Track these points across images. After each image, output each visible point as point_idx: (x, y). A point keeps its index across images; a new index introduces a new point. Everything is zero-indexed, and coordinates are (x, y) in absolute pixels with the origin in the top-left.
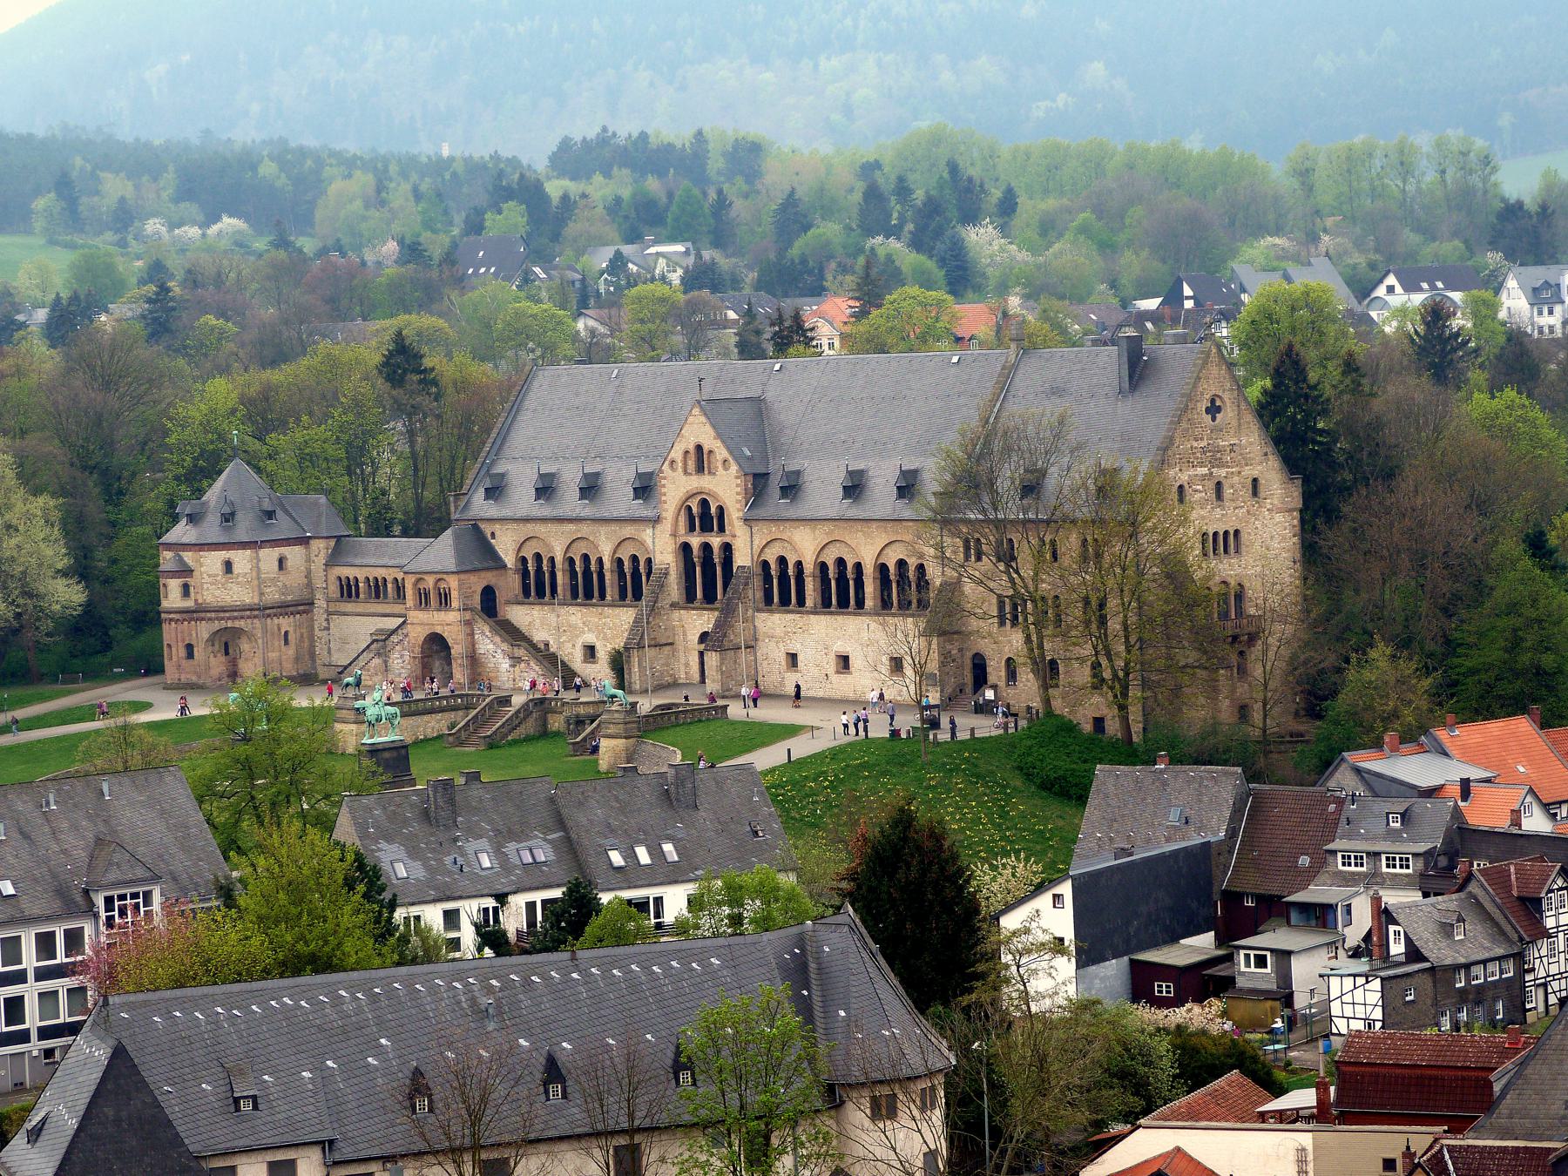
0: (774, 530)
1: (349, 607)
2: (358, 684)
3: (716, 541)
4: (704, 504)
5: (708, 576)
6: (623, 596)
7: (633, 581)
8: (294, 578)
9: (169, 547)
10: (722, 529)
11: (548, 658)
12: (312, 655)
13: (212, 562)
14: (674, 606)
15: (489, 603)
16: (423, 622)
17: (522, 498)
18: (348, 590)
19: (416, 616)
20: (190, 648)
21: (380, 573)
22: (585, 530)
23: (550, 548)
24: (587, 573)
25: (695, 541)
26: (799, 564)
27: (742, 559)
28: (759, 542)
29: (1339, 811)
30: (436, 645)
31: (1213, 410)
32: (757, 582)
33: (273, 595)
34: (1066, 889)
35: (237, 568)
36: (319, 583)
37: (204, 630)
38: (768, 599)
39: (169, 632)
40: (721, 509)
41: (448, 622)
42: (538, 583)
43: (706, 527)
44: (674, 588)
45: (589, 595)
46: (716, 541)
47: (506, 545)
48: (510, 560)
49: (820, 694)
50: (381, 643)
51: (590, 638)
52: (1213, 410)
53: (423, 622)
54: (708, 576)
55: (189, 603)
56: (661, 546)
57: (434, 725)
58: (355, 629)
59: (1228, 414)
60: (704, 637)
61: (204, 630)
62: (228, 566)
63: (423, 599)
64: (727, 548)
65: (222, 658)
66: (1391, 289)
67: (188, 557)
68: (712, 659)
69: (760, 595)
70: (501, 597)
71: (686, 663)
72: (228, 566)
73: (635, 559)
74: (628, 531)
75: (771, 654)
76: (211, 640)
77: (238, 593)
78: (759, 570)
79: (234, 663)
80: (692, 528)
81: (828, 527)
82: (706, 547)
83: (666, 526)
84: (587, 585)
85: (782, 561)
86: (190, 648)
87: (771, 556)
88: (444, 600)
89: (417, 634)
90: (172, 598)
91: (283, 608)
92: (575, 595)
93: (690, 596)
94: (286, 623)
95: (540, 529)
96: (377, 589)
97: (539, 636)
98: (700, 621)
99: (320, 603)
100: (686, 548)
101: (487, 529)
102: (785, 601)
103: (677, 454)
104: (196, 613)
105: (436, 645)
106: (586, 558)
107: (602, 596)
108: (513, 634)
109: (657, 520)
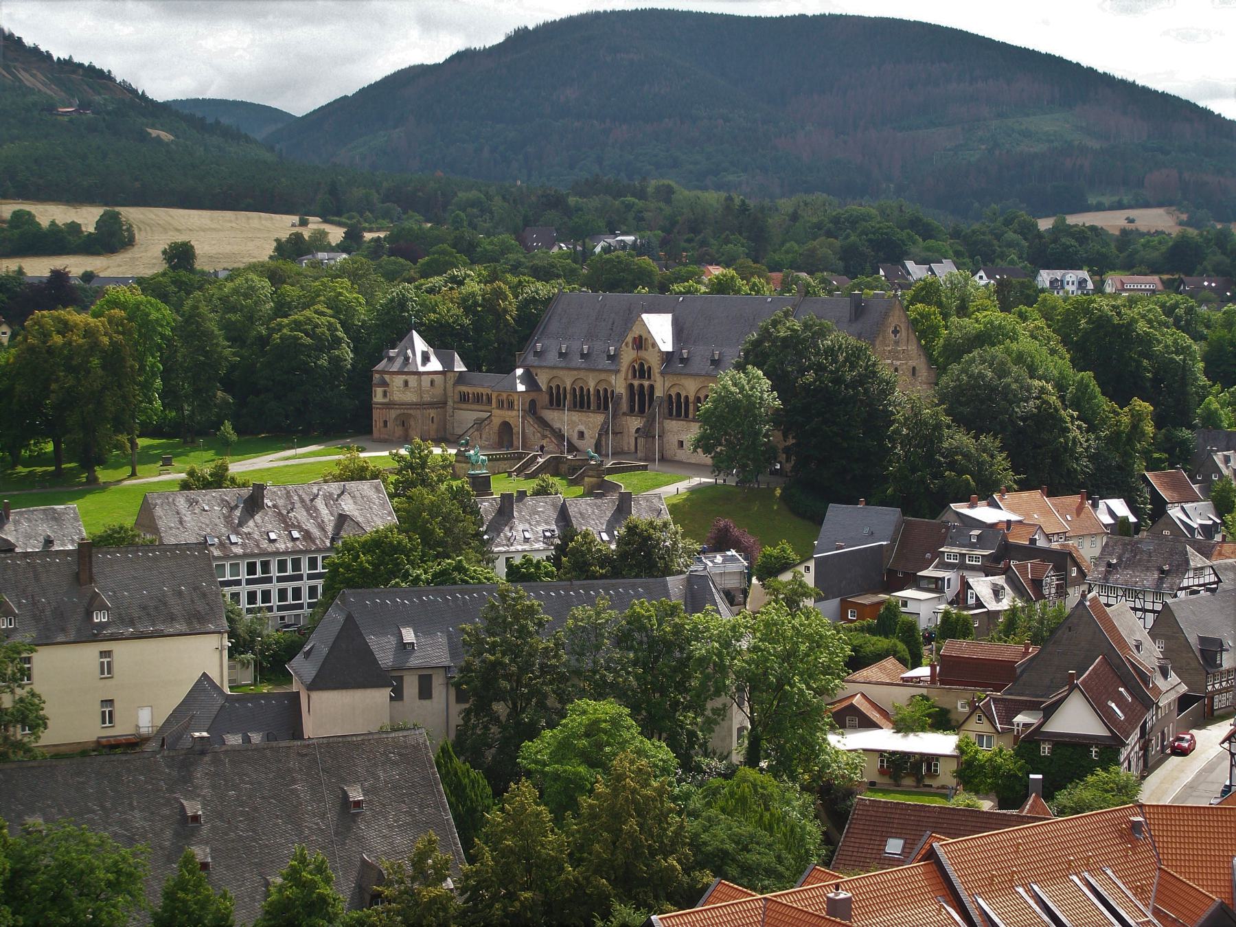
0: (675, 380)
1: (464, 406)
2: (467, 444)
3: (646, 383)
4: (642, 365)
5: (641, 400)
6: (599, 408)
7: (604, 401)
8: (438, 391)
9: (378, 372)
10: (649, 377)
11: (559, 436)
12: (445, 429)
13: (398, 381)
14: (624, 414)
15: (532, 409)
16: (499, 416)
17: (552, 358)
18: (464, 398)
19: (496, 412)
20: (385, 422)
21: (480, 390)
22: (582, 374)
23: (564, 382)
24: (582, 395)
25: (636, 383)
26: (687, 397)
27: (658, 393)
28: (667, 385)
29: (947, 532)
30: (506, 428)
31: (895, 332)
32: (665, 405)
33: (427, 398)
34: (812, 564)
35: (410, 384)
36: (450, 394)
37: (393, 414)
38: (671, 414)
39: (377, 415)
40: (649, 368)
41: (514, 417)
42: (556, 399)
43: (642, 376)
44: (624, 406)
45: (582, 406)
46: (646, 383)
47: (542, 380)
48: (544, 388)
49: (693, 461)
50: (479, 424)
51: (582, 428)
52: (895, 332)
53: (499, 416)
54: (641, 400)
55: (387, 400)
56: (619, 385)
57: (503, 465)
58: (468, 416)
59: (904, 333)
60: (638, 430)
61: (393, 414)
62: (406, 383)
63: (501, 405)
64: (652, 387)
65: (400, 428)
66: (981, 278)
67: (387, 377)
68: (641, 441)
69: (666, 411)
70: (538, 406)
71: (629, 442)
72: (406, 383)
73: (606, 390)
74: (603, 376)
75: (672, 440)
76: (396, 419)
77: (410, 397)
78: (666, 398)
79: (407, 430)
80: (635, 376)
81: (702, 379)
82: (641, 386)
83: (623, 374)
84: (581, 402)
85: (678, 395)
86: (385, 422)
87: (673, 393)
88: (511, 406)
89: (497, 421)
90: (378, 396)
91: (431, 405)
92: (575, 406)
93: (632, 409)
94: (433, 413)
95: (561, 373)
96: (478, 399)
97: (556, 425)
98: (635, 423)
99: (450, 403)
100: (631, 386)
101: (534, 371)
102: (679, 415)
103: (629, 339)
104: (390, 405)
105: (506, 428)
106: (582, 388)
107: (589, 407)
108: (544, 424)
109: (618, 371)
